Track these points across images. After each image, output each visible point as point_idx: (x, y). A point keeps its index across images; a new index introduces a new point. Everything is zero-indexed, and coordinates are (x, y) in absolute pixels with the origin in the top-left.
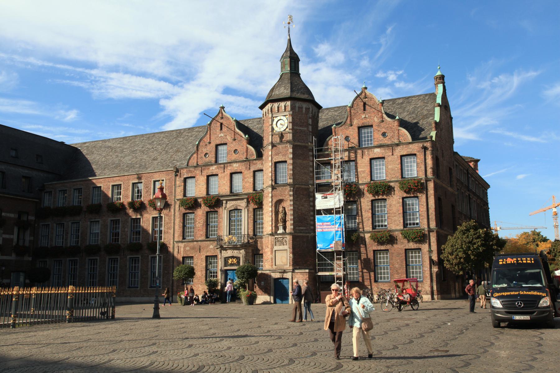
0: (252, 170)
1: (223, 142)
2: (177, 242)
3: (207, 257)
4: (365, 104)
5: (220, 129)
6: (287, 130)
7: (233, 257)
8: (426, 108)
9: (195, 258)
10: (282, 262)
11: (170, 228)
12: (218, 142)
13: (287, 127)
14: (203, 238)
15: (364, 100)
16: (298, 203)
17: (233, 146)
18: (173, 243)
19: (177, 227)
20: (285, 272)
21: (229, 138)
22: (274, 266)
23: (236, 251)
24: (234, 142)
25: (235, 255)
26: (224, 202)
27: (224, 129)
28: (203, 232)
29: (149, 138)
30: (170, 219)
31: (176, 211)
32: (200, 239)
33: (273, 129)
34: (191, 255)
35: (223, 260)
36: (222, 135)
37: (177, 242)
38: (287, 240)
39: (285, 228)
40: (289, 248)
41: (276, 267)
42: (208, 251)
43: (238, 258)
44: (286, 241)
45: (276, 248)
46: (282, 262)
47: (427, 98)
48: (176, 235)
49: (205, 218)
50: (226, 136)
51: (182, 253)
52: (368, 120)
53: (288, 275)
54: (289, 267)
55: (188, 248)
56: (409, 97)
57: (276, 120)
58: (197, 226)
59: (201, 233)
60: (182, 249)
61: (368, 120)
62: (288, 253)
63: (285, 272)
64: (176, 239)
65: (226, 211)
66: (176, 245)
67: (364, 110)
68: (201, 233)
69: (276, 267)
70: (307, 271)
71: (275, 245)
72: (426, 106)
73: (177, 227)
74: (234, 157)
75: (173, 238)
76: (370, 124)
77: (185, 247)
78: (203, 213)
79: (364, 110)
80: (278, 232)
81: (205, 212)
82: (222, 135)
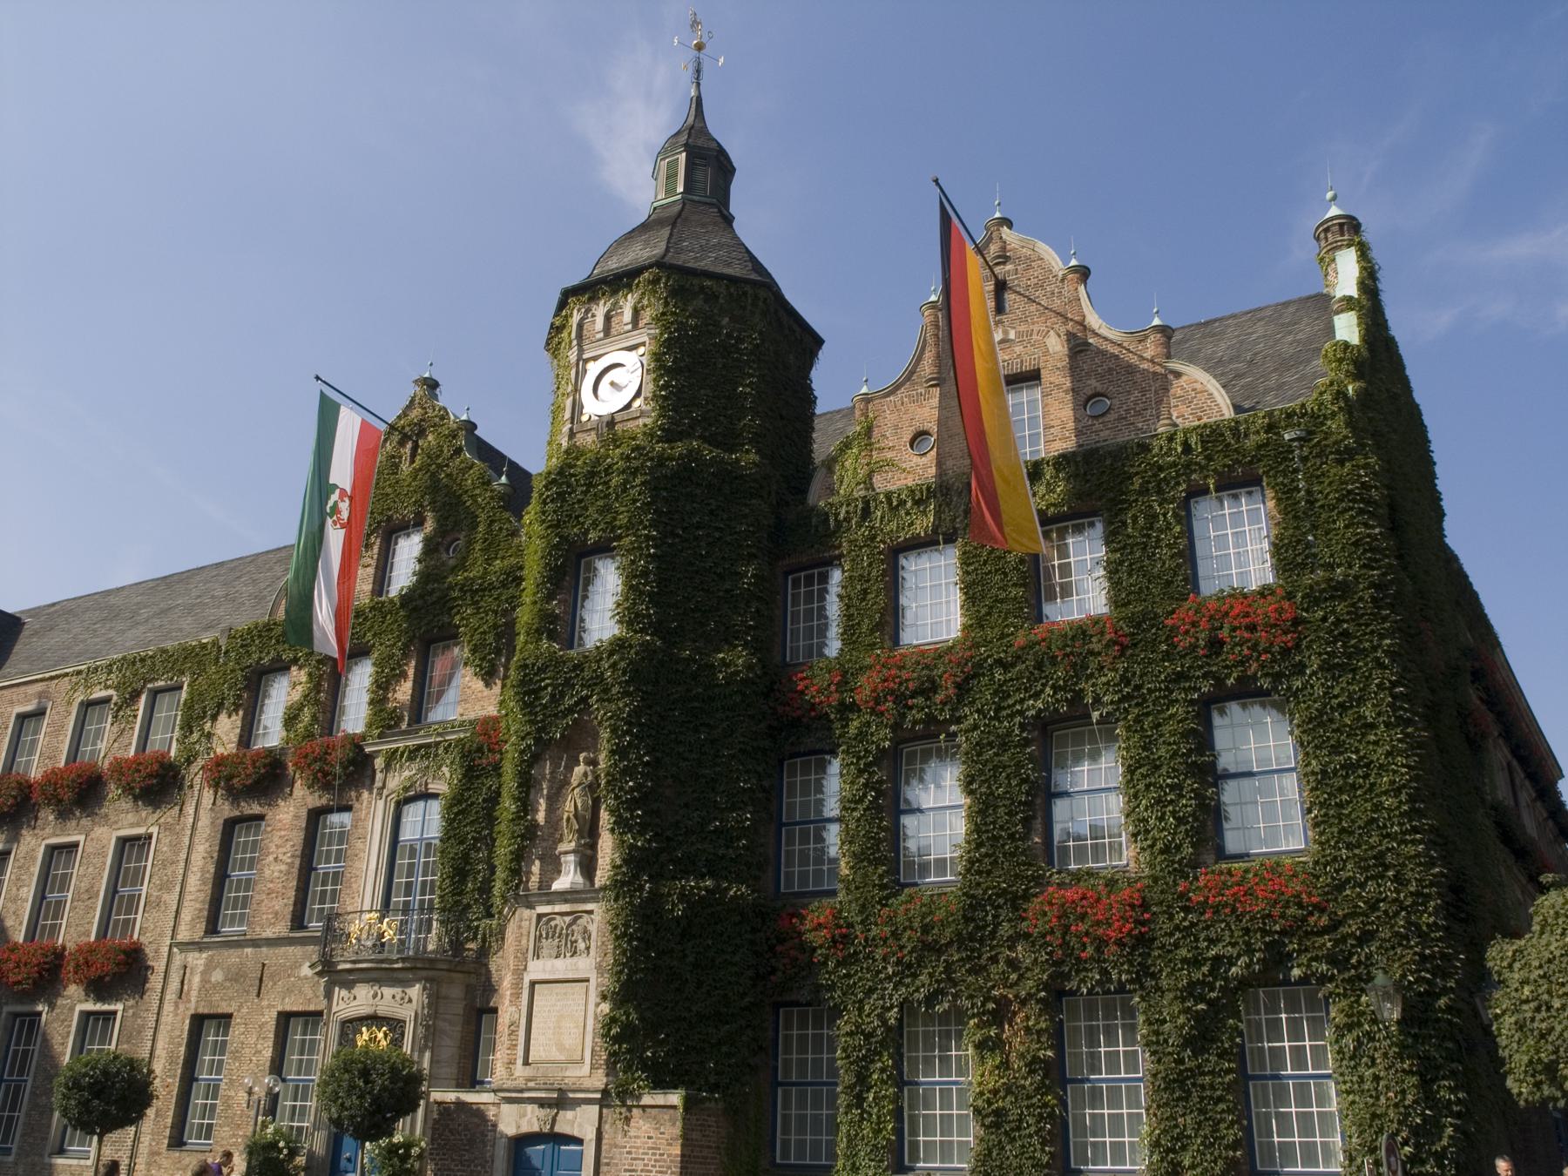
2: (186, 946)
3: (285, 1019)
4: (1001, 287)
6: (637, 403)
7: (374, 1020)
8: (1290, 338)
9: (236, 1020)
10: (561, 1048)
11: (166, 887)
13: (638, 394)
14: (281, 929)
15: (997, 270)
19: (194, 881)
20: (561, 1101)
22: (519, 1070)
23: (388, 992)
25: (382, 1010)
26: (379, 763)
28: (283, 904)
29: (232, 569)
30: (175, 847)
31: (203, 809)
32: (269, 933)
33: (577, 407)
34: (224, 1008)
35: (334, 1031)
37: (186, 946)
38: (593, 928)
39: (588, 866)
40: (599, 967)
41: (528, 1072)
42: (289, 991)
43: (395, 1025)
44: (586, 935)
45: (537, 969)
46: (561, 1048)
47: (1291, 309)
48: (186, 916)
49: (298, 837)
51: (194, 993)
52: (1018, 349)
53: (581, 1122)
54: (589, 1076)
55: (217, 976)
56: (1207, 323)
57: (594, 369)
58: (267, 872)
60: (197, 979)
61: (1018, 349)
62: (593, 997)
63: (561, 1101)
64: (183, 935)
65: (381, 804)
67: (1000, 309)
69: (528, 1072)
70: (675, 1098)
71: (537, 955)
72: (1290, 333)
73: (194, 881)
76: (1027, 367)
77: (209, 967)
78: (296, 817)
79: (1000, 309)
80: (556, 886)
81: (304, 813)
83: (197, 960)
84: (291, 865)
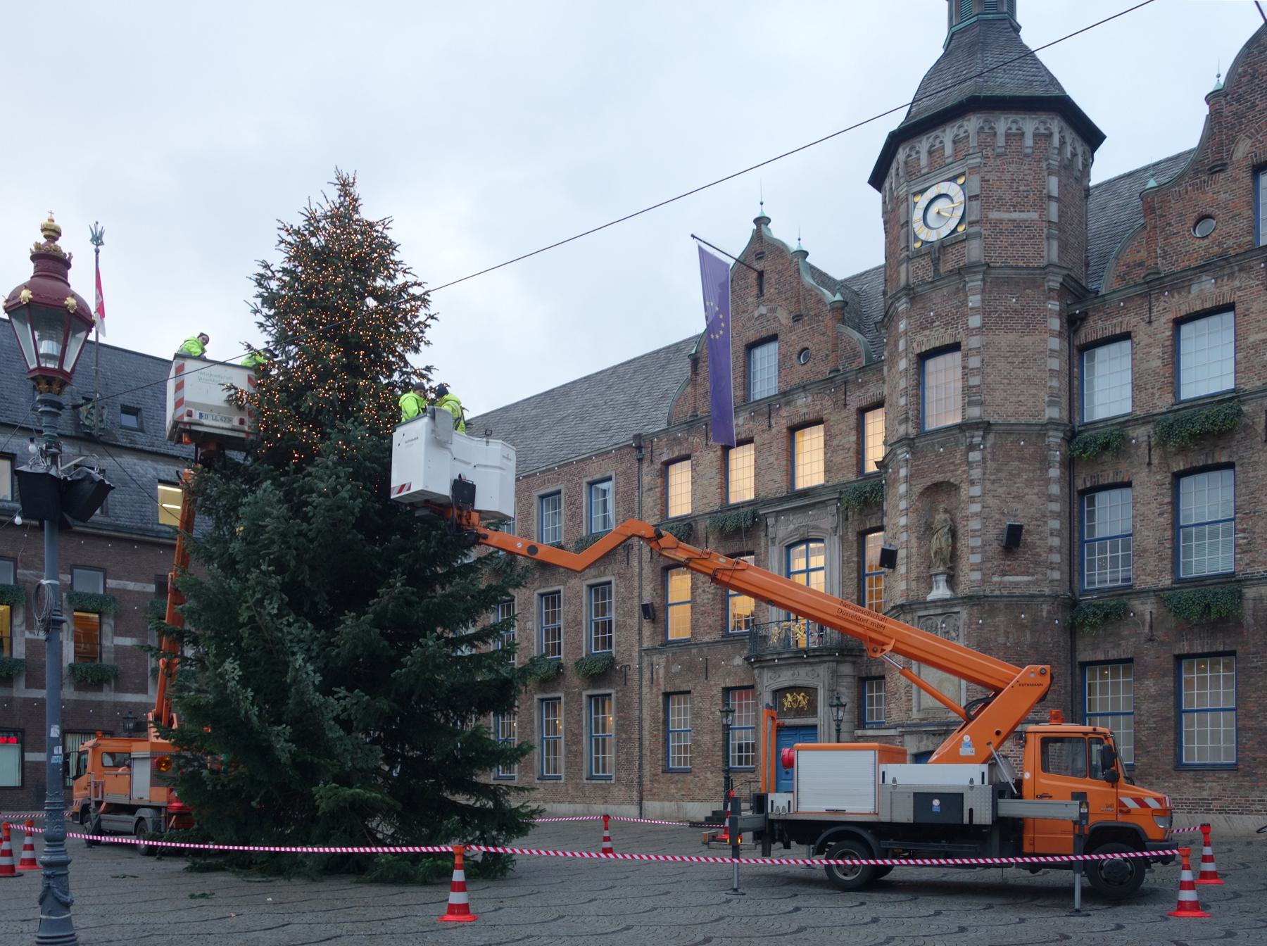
0: (854, 404)
1: (764, 334)
5: (755, 291)
12: (752, 336)
14: (715, 636)
16: (1000, 490)
17: (797, 338)
18: (641, 657)
21: (783, 316)
24: (799, 328)
27: (769, 291)
32: (707, 639)
36: (763, 310)
50: (773, 310)
59: (710, 621)
60: (662, 672)
64: (645, 646)
66: (645, 664)
68: (710, 621)
74: (800, 372)
75: (640, 640)
82: (763, 310)
83: (660, 660)
84: (715, 594)
